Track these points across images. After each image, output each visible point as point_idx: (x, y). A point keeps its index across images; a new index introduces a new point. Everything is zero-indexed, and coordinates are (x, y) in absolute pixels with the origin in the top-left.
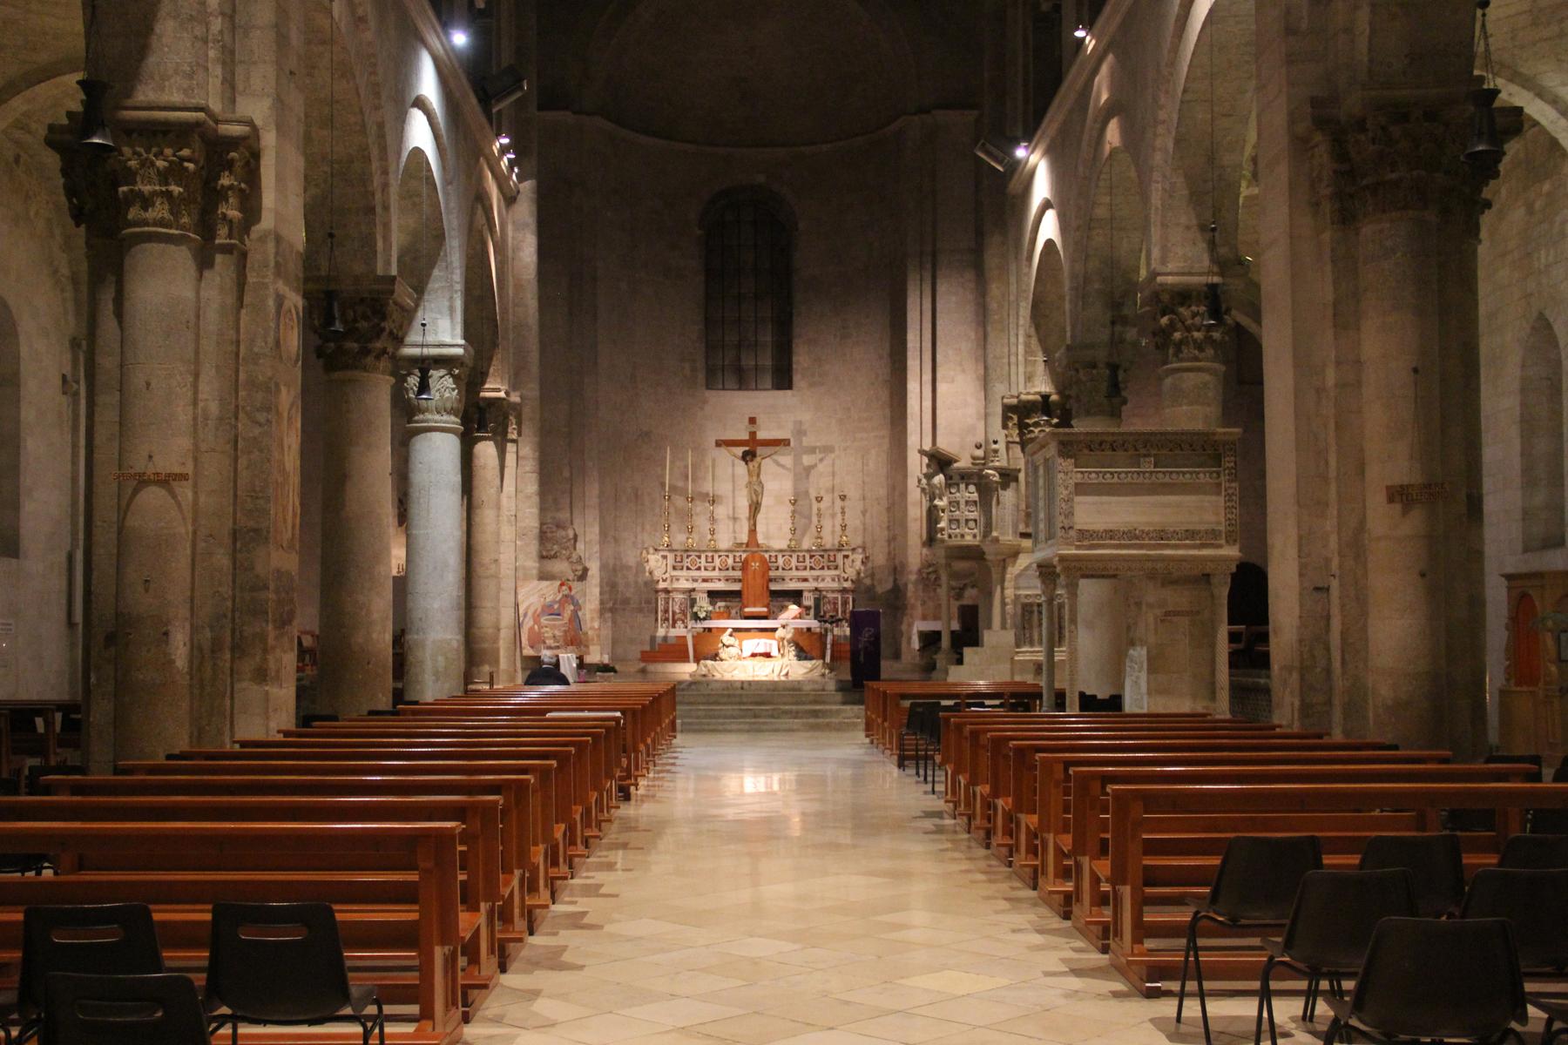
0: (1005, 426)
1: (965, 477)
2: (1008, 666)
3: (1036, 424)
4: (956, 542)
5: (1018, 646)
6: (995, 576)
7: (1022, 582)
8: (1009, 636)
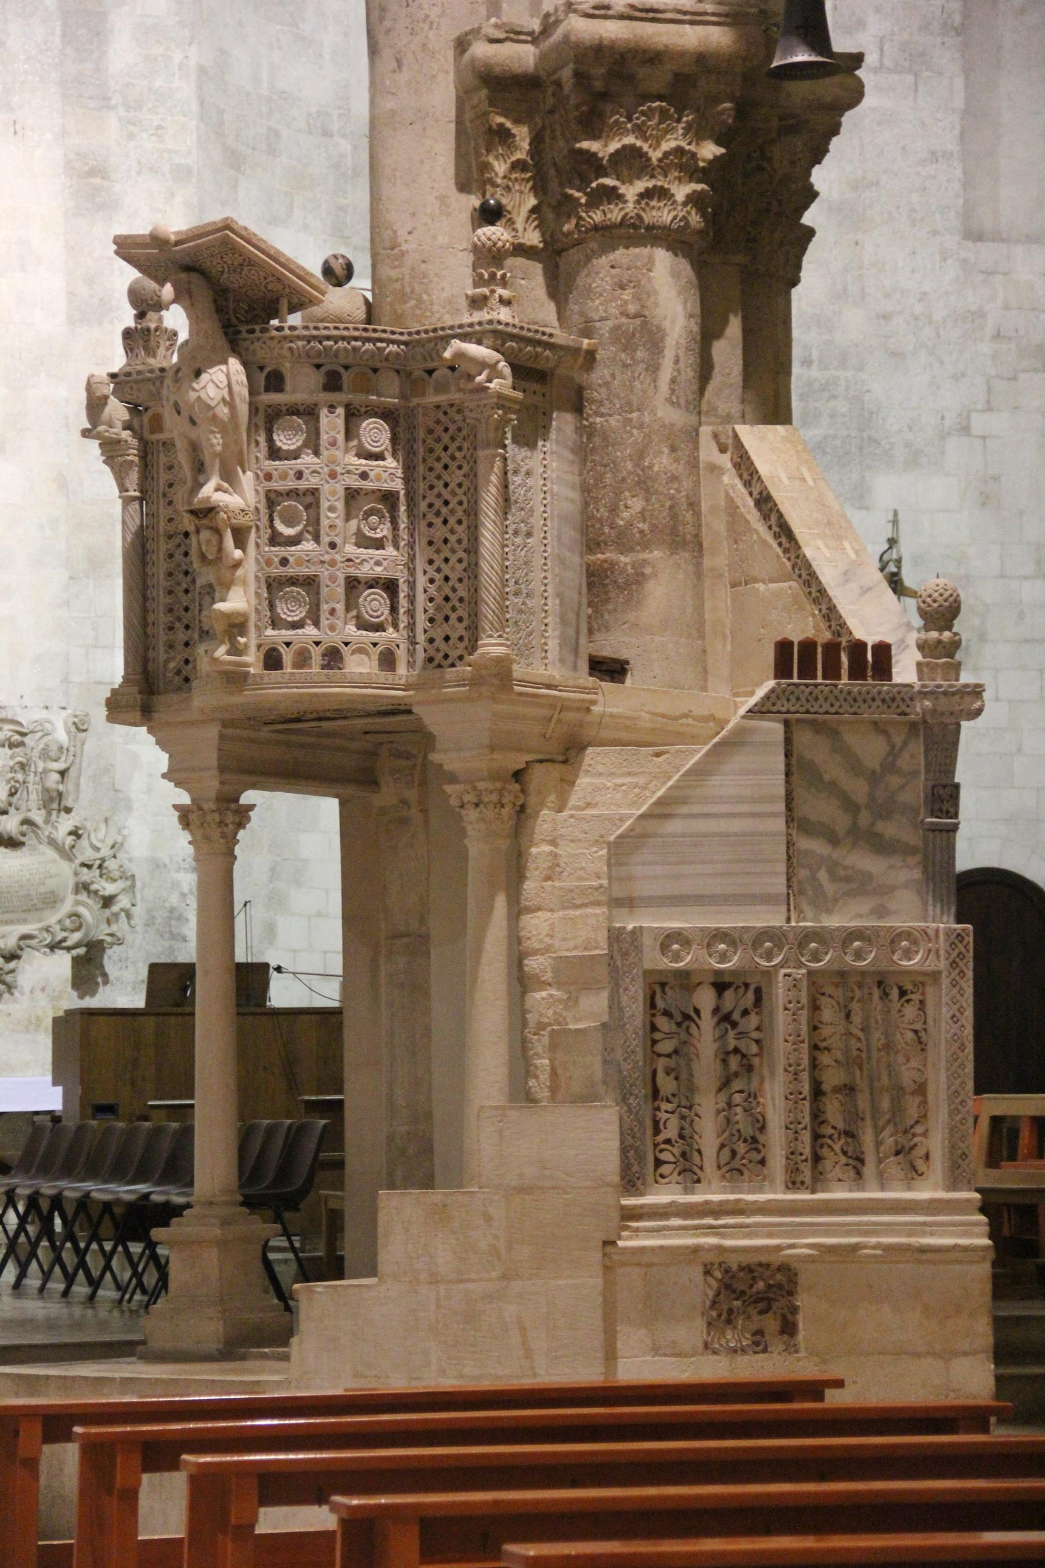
0: (470, 176)
1: (347, 375)
2: (592, 1281)
3: (630, 161)
4: (287, 688)
5: (631, 1183)
6: (480, 844)
7: (648, 874)
8: (593, 1136)
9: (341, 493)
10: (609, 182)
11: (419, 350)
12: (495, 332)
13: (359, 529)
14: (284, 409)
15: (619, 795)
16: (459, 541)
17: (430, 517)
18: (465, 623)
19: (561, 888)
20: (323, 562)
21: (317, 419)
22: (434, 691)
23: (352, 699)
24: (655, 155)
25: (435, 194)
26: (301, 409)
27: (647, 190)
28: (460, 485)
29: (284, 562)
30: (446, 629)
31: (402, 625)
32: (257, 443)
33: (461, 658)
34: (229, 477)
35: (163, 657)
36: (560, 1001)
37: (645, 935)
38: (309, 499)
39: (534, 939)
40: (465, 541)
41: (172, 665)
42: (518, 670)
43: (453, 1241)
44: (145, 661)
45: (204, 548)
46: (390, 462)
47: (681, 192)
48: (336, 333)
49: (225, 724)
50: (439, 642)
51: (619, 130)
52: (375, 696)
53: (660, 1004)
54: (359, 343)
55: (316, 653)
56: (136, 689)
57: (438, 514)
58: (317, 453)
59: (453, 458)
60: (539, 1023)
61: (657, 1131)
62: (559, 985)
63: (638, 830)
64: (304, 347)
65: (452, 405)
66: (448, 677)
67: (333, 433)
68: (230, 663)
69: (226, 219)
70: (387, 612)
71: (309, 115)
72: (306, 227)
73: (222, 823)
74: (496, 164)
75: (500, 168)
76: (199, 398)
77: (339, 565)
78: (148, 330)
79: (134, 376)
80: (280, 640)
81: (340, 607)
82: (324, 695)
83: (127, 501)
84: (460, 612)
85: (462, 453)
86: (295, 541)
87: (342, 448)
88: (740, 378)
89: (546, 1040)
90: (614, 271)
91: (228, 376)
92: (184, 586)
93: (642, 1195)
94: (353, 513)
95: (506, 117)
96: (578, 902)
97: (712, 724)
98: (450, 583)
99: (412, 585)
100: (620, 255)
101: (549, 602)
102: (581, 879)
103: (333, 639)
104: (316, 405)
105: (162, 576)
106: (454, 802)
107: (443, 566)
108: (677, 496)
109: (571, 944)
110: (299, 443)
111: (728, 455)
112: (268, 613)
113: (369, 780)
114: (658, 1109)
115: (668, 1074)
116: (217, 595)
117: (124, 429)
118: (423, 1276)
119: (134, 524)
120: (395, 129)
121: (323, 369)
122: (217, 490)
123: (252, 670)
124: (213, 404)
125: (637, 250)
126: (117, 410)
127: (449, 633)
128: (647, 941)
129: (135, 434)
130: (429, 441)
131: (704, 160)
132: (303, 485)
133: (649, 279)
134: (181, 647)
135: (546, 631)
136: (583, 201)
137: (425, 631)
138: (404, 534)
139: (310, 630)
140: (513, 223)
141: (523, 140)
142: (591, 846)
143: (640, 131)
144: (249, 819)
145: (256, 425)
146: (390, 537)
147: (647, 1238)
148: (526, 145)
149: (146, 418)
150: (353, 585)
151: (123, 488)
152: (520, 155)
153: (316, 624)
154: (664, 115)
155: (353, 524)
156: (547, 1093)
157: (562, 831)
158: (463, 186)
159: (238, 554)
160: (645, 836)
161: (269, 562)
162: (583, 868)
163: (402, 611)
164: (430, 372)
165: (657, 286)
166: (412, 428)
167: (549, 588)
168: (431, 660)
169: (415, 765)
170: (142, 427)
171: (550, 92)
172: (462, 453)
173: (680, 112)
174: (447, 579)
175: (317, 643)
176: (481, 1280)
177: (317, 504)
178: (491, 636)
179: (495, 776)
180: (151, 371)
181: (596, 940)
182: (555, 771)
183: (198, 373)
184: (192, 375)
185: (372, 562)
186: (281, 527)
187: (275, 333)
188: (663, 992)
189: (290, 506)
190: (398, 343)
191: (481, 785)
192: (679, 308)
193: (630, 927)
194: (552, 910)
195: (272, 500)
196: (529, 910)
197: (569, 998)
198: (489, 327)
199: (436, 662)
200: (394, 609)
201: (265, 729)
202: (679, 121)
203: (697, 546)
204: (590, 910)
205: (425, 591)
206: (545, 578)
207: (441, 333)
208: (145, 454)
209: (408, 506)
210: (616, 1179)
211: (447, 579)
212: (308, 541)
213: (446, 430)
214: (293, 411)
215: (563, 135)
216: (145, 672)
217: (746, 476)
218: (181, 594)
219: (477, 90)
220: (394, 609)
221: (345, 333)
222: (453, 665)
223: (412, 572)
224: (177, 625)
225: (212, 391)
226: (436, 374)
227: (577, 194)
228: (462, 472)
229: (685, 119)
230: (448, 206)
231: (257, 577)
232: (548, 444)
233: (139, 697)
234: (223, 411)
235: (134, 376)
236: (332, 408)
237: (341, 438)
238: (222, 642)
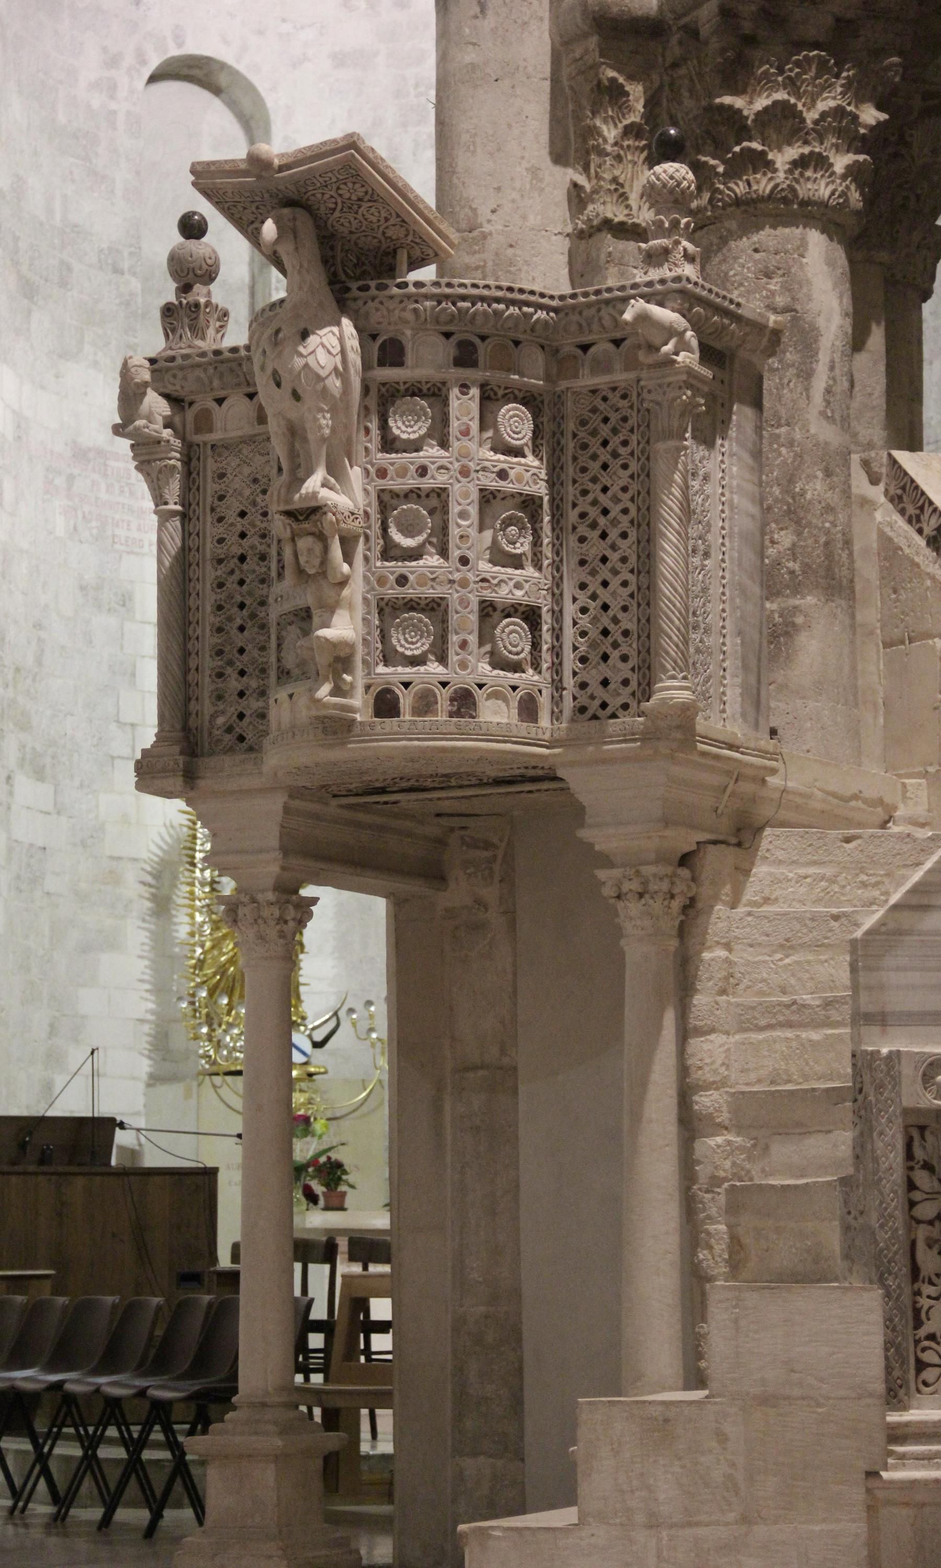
0: (571, 143)
1: (490, 345)
6: (641, 945)
9: (475, 495)
10: (756, 145)
11: (575, 317)
12: (683, 292)
13: (495, 541)
14: (402, 388)
15: (802, 890)
16: (624, 560)
17: (583, 530)
18: (630, 664)
19: (738, 1005)
20: (451, 582)
21: (445, 402)
22: (591, 748)
23: (483, 757)
24: (810, 116)
25: (525, 164)
26: (425, 388)
27: (802, 156)
28: (625, 489)
29: (402, 580)
30: (605, 670)
31: (545, 666)
32: (367, 431)
33: (625, 707)
34: (335, 470)
35: (207, 707)
36: (741, 1148)
37: (903, 1062)
38: (434, 502)
39: (707, 1069)
40: (633, 559)
41: (220, 720)
42: (701, 724)
43: (679, 1470)
44: (186, 715)
45: (302, 560)
46: (531, 460)
47: (841, 162)
48: (475, 291)
49: (295, 793)
50: (595, 687)
51: (768, 83)
52: (516, 753)
53: (919, 1153)
54: (502, 306)
55: (443, 696)
56: (177, 749)
57: (594, 525)
58: (444, 444)
59: (615, 455)
60: (713, 1177)
61: (918, 1324)
62: (740, 1129)
63: (891, 925)
64: (433, 308)
65: (614, 389)
66: (610, 730)
67: (465, 419)
68: (336, 706)
69: (351, 135)
70: (528, 648)
71: (101, 251)
72: (96, 363)
73: (282, 920)
74: (604, 128)
75: (611, 133)
76: (306, 365)
77: (472, 585)
78: (197, 305)
79: (179, 361)
80: (396, 679)
81: (473, 639)
82: (454, 749)
83: (164, 517)
84: (624, 649)
85: (628, 449)
86: (415, 554)
87: (476, 439)
88: (884, 399)
89: (722, 1199)
90: (757, 256)
91: (341, 340)
92: (239, 622)
93: (905, 1408)
94: (488, 521)
95: (619, 71)
96: (763, 1022)
97: (879, 809)
98: (611, 613)
99: (557, 616)
100: (767, 236)
101: (728, 641)
102: (761, 993)
103: (462, 679)
104: (444, 383)
105: (209, 609)
106: (608, 891)
107: (600, 591)
108: (833, 531)
109: (753, 1076)
110: (423, 431)
111: (882, 487)
112: (379, 645)
113: (435, 875)
114: (918, 1293)
115: (930, 1247)
116: (316, 620)
117: (165, 427)
118: (640, 1518)
119: (174, 544)
120: (475, 87)
121: (453, 340)
122: (323, 485)
123: (358, 717)
124: (323, 373)
125: (787, 230)
126: (155, 404)
127: (609, 674)
128: (907, 1070)
129: (177, 434)
131: (865, 126)
132: (427, 483)
133: (802, 266)
135: (724, 677)
136: (721, 169)
137: (575, 674)
138: (547, 551)
139: (434, 668)
140: (627, 199)
141: (637, 101)
142: (775, 952)
143: (792, 85)
144: (310, 915)
145: (366, 408)
146: (530, 556)
147: (916, 1468)
148: (640, 107)
149: (190, 414)
150: (489, 611)
151: (159, 500)
152: (634, 118)
153: (442, 659)
154: (823, 67)
155: (488, 534)
156: (724, 1269)
157: (737, 932)
158: (559, 157)
159: (345, 568)
160: (899, 932)
161: (381, 581)
162: (763, 980)
163: (545, 647)
164: (585, 348)
165: (810, 275)
166: (559, 418)
167: (727, 623)
168: (582, 710)
169: (495, 857)
170: (184, 426)
171: (674, 40)
172: (628, 449)
173: (840, 64)
175: (444, 684)
176: (717, 1523)
177: (445, 510)
178: (673, 677)
179: (661, 859)
180: (203, 354)
181: (786, 1071)
182: (729, 855)
183: (305, 335)
184: (298, 337)
185: (511, 584)
186: (397, 537)
187: (395, 290)
188: (923, 1137)
189: (411, 509)
190: (548, 309)
191: (648, 870)
192: (835, 304)
193: (885, 1051)
194: (727, 1033)
195: (386, 502)
196: (700, 1032)
197: (754, 1146)
198: (676, 286)
199: (590, 712)
200: (536, 645)
201: (334, 802)
202: (837, 76)
203: (851, 596)
204: (778, 1033)
205: (575, 623)
206: (724, 611)
207: (606, 295)
208: (187, 460)
209: (553, 516)
210: (880, 1387)
211: (605, 607)
212: (431, 555)
213: (606, 420)
214: (415, 391)
215: (691, 91)
216: (186, 729)
217: (911, 510)
218: (234, 632)
219: (585, 36)
220: (536, 645)
221: (486, 292)
222: (613, 716)
223: (557, 598)
224: (229, 671)
225: (322, 356)
226: (592, 350)
227: (712, 162)
228: (628, 472)
229: (844, 74)
230: (541, 180)
231: (365, 599)
232: (726, 443)
233: (181, 759)
234: (335, 384)
235: (179, 361)
236: (464, 388)
237: (475, 426)
238: (326, 679)
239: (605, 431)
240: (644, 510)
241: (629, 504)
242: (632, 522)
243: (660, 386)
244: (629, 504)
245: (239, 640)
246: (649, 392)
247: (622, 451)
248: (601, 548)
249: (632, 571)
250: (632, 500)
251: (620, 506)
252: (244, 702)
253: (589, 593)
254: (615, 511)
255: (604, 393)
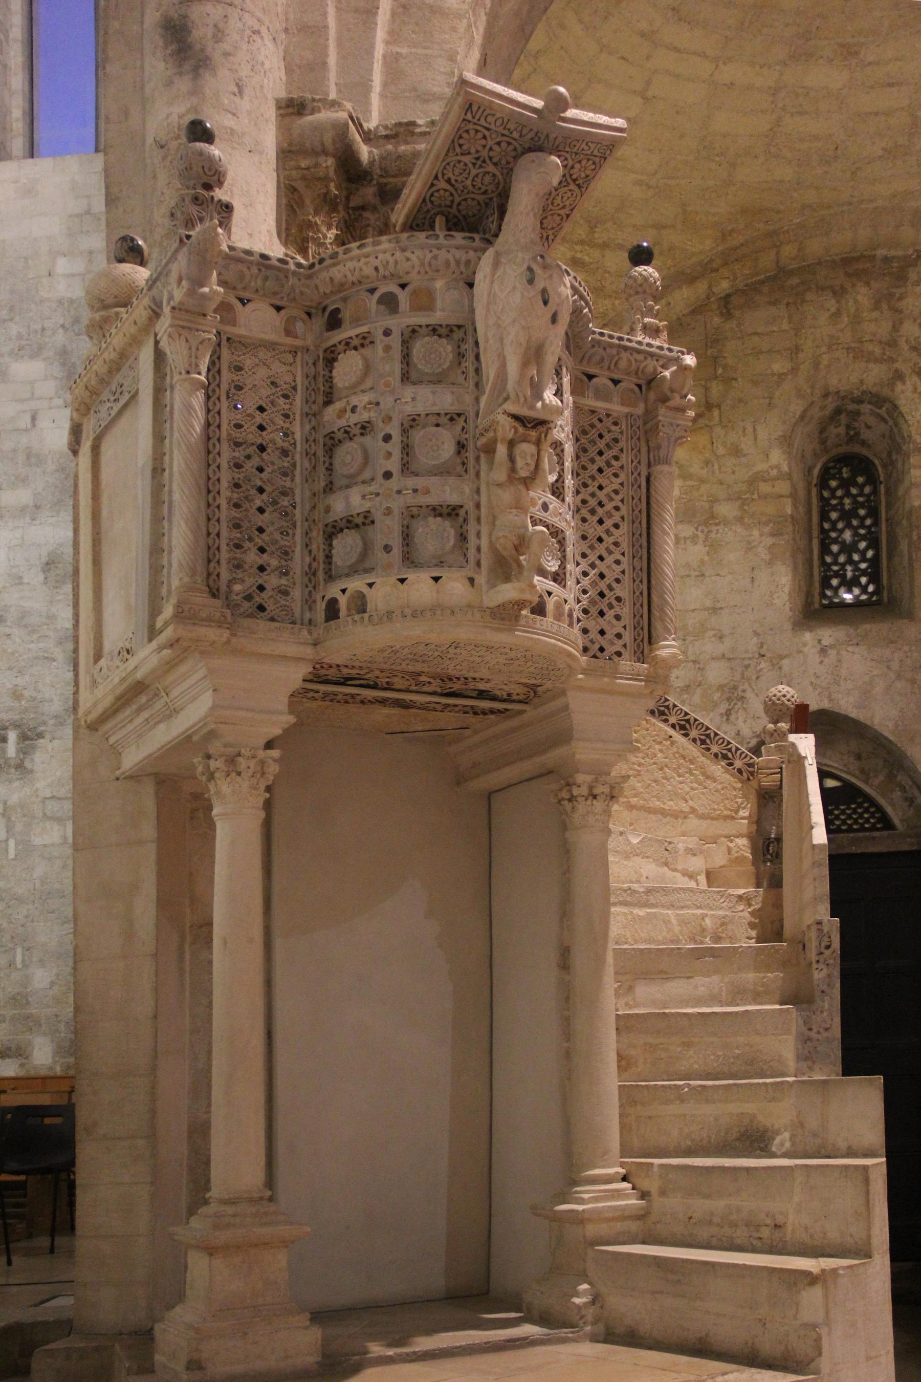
16: (616, 544)
28: (616, 492)
40: (625, 546)
59: (609, 465)
107: (598, 562)
130: (583, 441)
134: (255, 570)
164: (590, 377)
174: (602, 576)
211: (602, 576)
213: (601, 436)
224: (247, 544)
226: (595, 380)
228: (619, 480)
239: (601, 444)
240: (636, 512)
241: (620, 504)
242: (623, 518)
243: (672, 425)
244: (620, 504)
245: (261, 520)
246: (663, 426)
247: (614, 462)
248: (600, 531)
249: (623, 554)
250: (622, 501)
251: (613, 504)
252: (265, 576)
253: (590, 562)
254: (609, 506)
255: (601, 416)
